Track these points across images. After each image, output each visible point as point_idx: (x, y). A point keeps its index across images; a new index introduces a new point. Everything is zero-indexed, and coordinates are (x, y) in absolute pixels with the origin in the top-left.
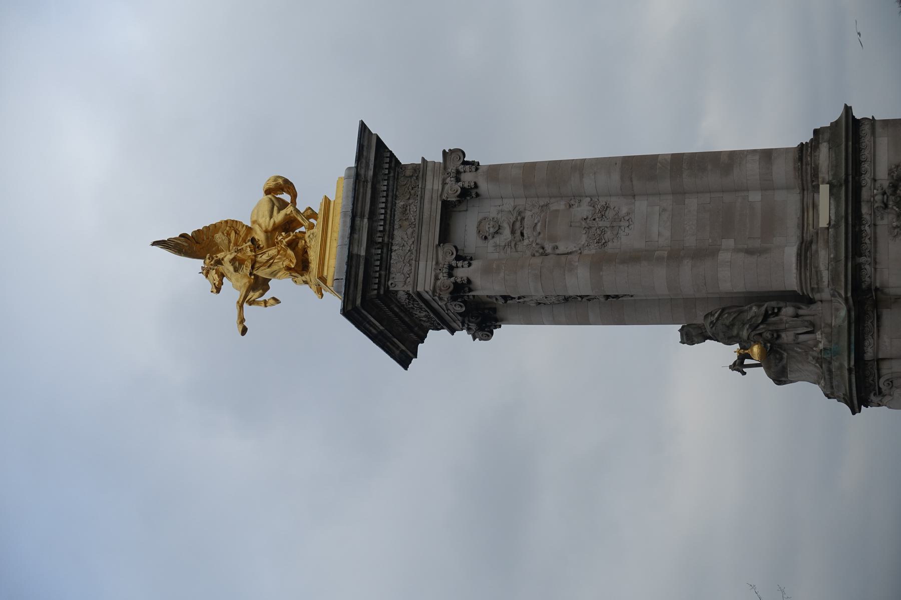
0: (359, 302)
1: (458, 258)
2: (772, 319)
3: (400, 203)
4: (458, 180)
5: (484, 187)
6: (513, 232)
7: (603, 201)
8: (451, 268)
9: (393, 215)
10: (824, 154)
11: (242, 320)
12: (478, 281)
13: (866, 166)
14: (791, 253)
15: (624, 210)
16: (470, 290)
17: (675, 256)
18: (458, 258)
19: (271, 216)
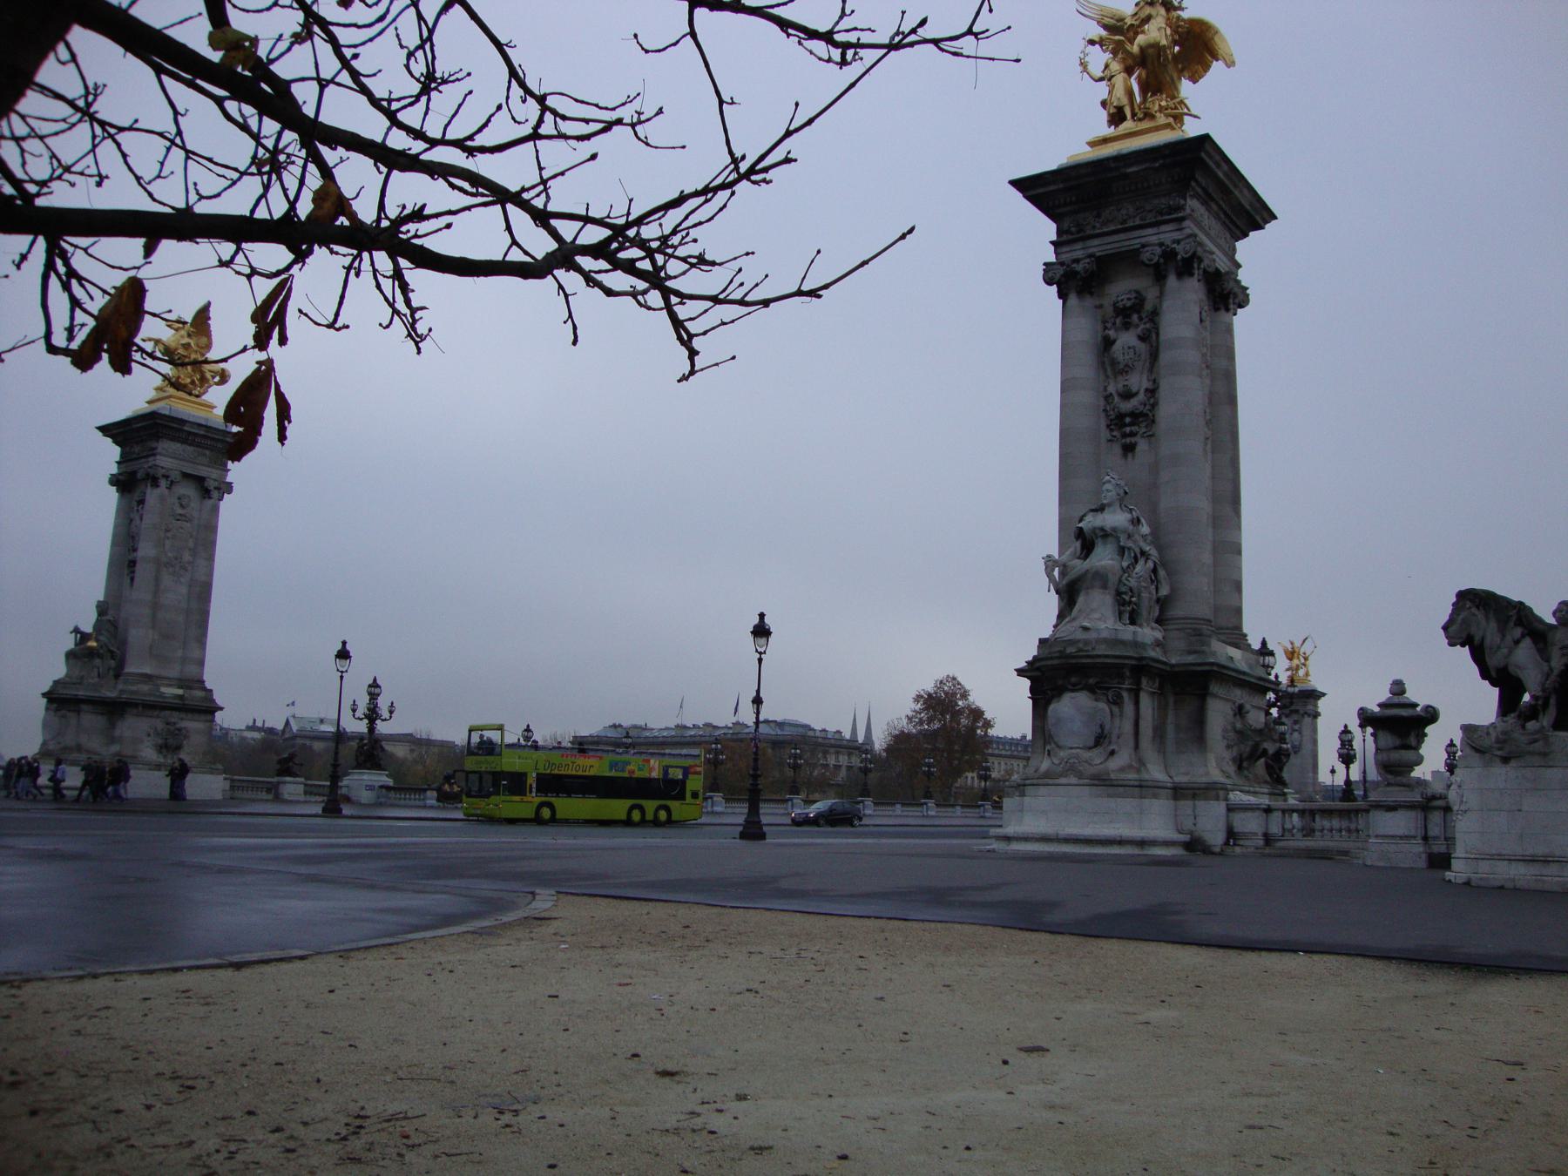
0: (158, 421)
1: (172, 482)
2: (109, 654)
3: (208, 452)
4: (215, 488)
5: (210, 503)
6: (181, 515)
7: (190, 568)
9: (204, 448)
10: (200, 694)
12: (157, 491)
13: (190, 716)
14: (147, 670)
15: (182, 580)
17: (156, 606)
18: (172, 482)
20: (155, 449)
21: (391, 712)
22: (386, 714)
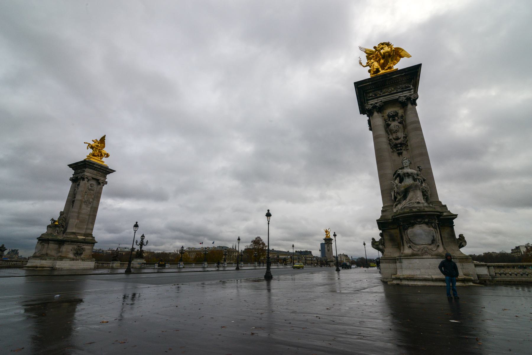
0: (86, 163)
1: (89, 180)
2: (62, 227)
3: (101, 173)
4: (102, 183)
5: (99, 186)
6: (90, 189)
7: (92, 203)
8: (87, 178)
10: (91, 238)
11: (87, 143)
12: (84, 182)
13: (86, 244)
14: (74, 231)
15: (89, 206)
16: (82, 180)
17: (79, 213)
18: (89, 180)
19: (104, 153)
20: (85, 170)
21: (147, 243)
22: (145, 244)
